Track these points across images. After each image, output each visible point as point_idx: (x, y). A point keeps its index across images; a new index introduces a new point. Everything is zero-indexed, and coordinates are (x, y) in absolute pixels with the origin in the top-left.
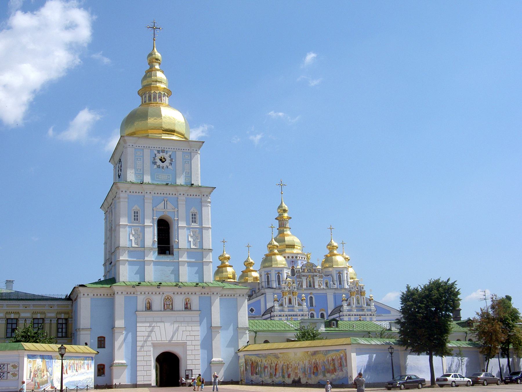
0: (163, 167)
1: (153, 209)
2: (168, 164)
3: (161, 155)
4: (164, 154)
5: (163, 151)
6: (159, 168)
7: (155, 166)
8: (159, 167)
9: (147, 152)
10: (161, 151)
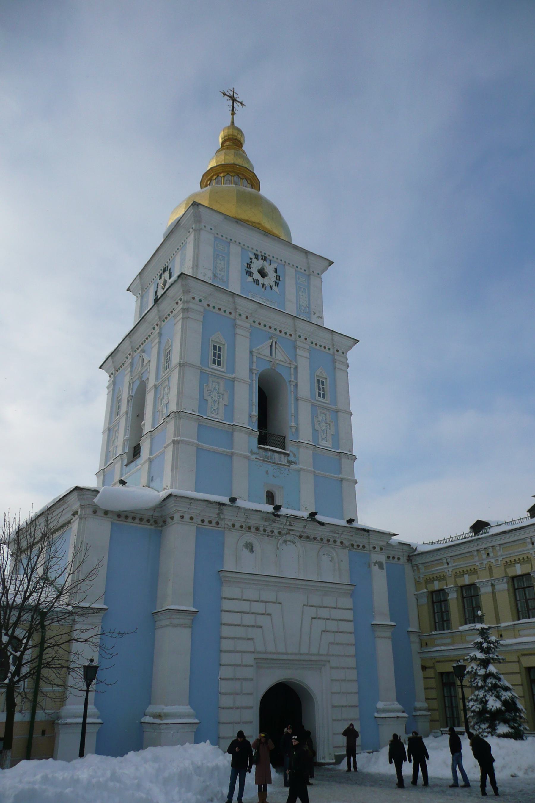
0: (264, 285)
1: (251, 352)
2: (273, 284)
3: (261, 262)
4: (266, 264)
5: (265, 259)
6: (258, 284)
7: (250, 279)
8: (256, 282)
9: (235, 250)
10: (260, 258)
